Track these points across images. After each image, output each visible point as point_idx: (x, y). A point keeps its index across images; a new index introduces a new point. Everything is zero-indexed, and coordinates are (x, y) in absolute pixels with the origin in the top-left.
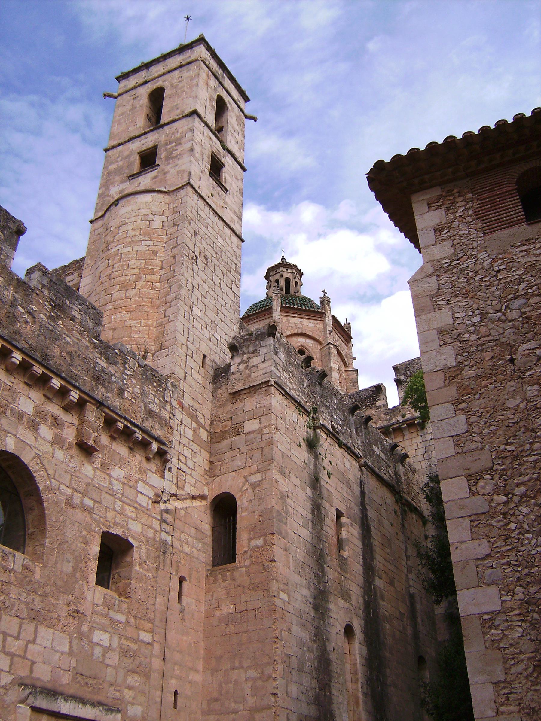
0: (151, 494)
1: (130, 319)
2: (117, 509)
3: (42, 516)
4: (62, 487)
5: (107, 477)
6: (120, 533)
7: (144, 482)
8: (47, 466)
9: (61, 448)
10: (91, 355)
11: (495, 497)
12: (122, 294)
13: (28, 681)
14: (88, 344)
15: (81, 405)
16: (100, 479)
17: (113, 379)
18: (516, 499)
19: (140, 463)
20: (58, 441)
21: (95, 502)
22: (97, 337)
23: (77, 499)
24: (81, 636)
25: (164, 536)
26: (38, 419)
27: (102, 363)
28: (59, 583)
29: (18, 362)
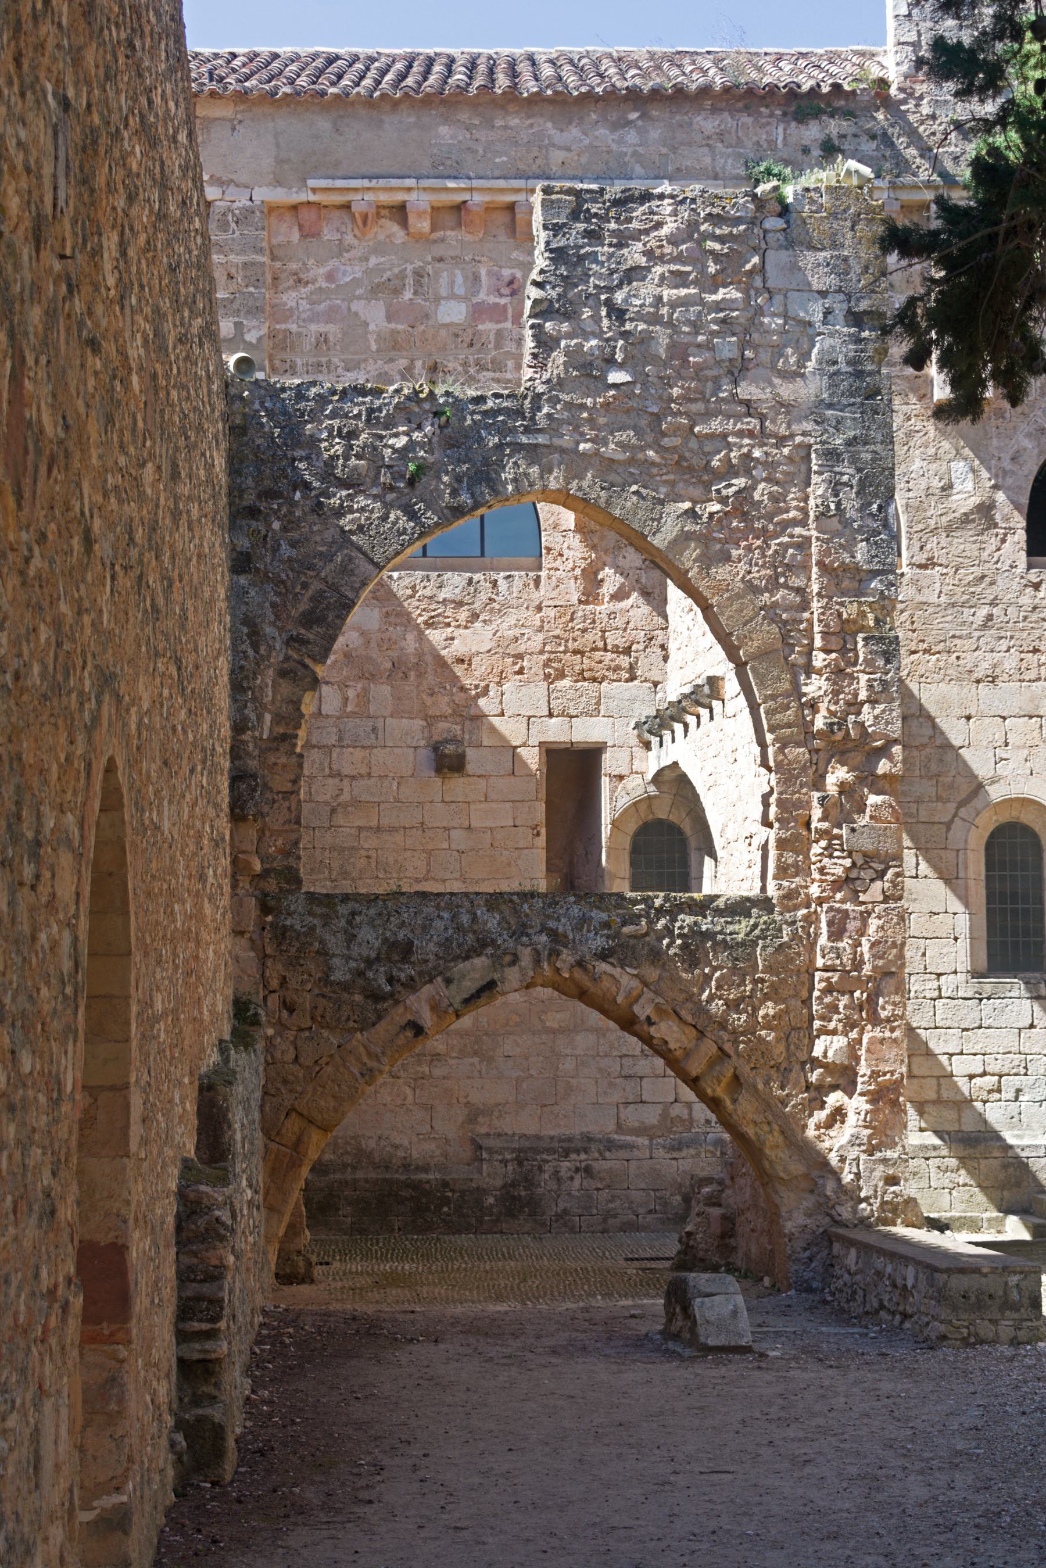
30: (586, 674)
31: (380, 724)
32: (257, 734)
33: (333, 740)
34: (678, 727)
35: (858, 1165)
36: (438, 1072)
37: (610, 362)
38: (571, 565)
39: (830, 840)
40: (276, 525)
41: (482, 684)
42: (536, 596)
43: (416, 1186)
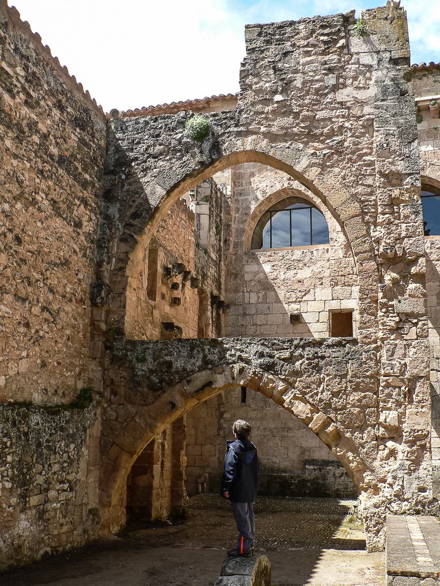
30: (346, 284)
33: (253, 312)
35: (403, 481)
36: (290, 435)
37: (275, 92)
38: (340, 244)
39: (387, 308)
41: (308, 289)
42: (327, 256)
43: (282, 477)
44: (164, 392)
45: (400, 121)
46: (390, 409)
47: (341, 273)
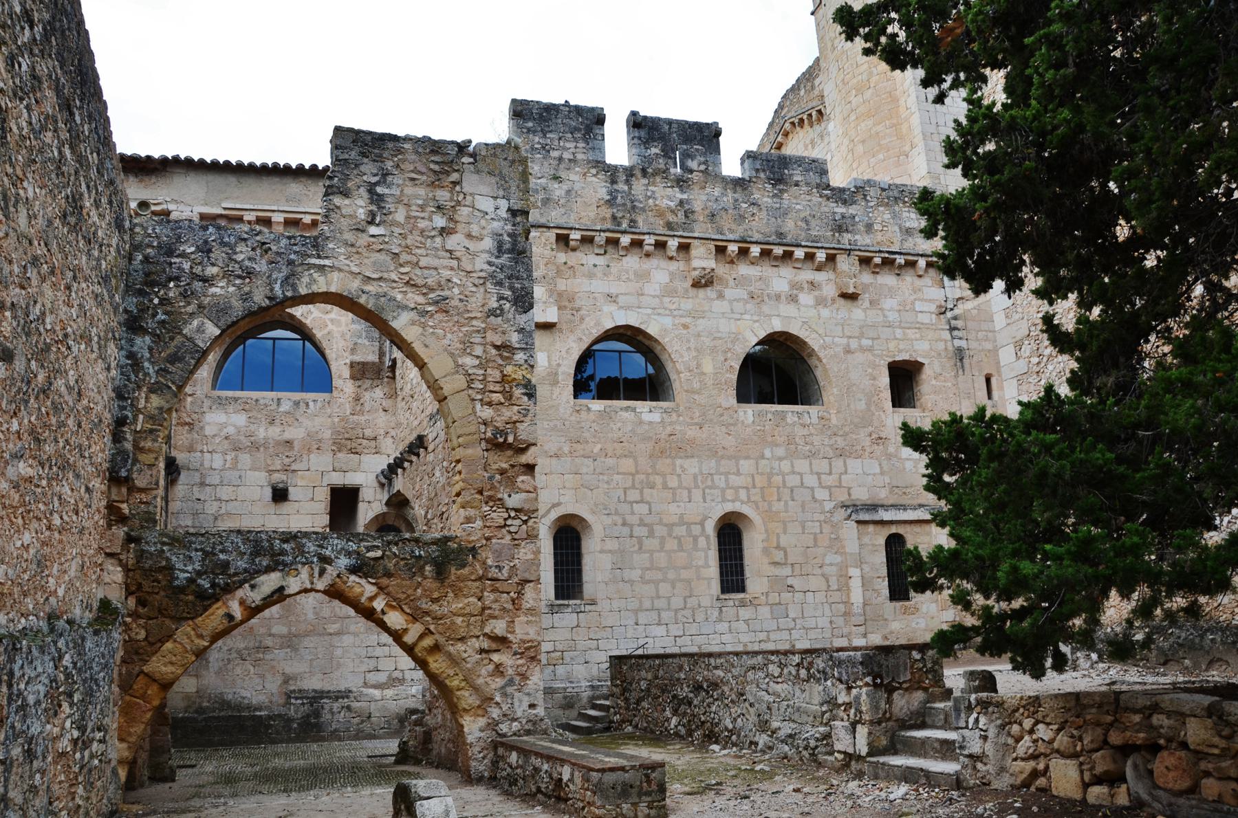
0: (933, 308)
1: (874, 125)
2: (898, 336)
3: (825, 370)
4: (836, 339)
5: (879, 312)
6: (907, 358)
7: (922, 300)
8: (816, 328)
9: (825, 306)
10: (826, 209)
11: (1032, 359)
12: (860, 99)
13: (847, 504)
14: (820, 199)
15: (831, 259)
16: (873, 316)
17: (857, 219)
18: (1045, 359)
19: (912, 284)
20: (820, 302)
21: (873, 339)
22: (828, 186)
23: (854, 344)
24: (889, 457)
25: (957, 343)
26: (795, 292)
27: (841, 210)
28: (856, 420)
29: (758, 255)
31: (243, 474)
32: (133, 427)
34: (400, 471)
36: (267, 657)
40: (156, 301)
44: (218, 600)
45: (516, 285)
46: (495, 618)
47: (347, 436)
